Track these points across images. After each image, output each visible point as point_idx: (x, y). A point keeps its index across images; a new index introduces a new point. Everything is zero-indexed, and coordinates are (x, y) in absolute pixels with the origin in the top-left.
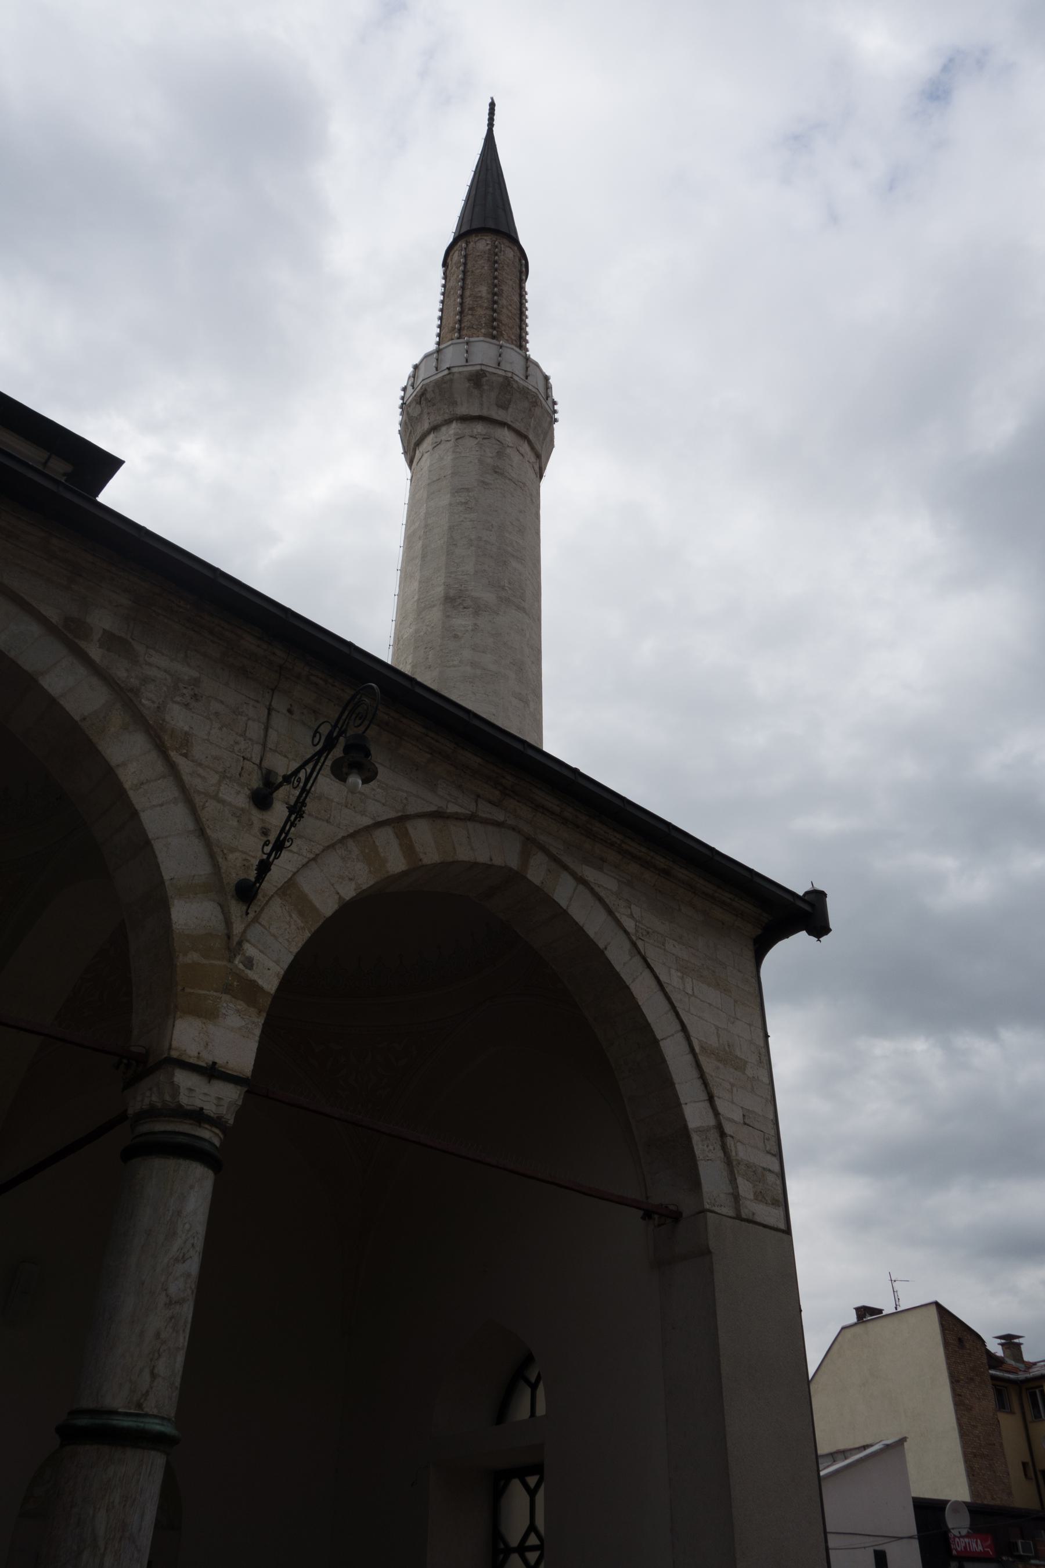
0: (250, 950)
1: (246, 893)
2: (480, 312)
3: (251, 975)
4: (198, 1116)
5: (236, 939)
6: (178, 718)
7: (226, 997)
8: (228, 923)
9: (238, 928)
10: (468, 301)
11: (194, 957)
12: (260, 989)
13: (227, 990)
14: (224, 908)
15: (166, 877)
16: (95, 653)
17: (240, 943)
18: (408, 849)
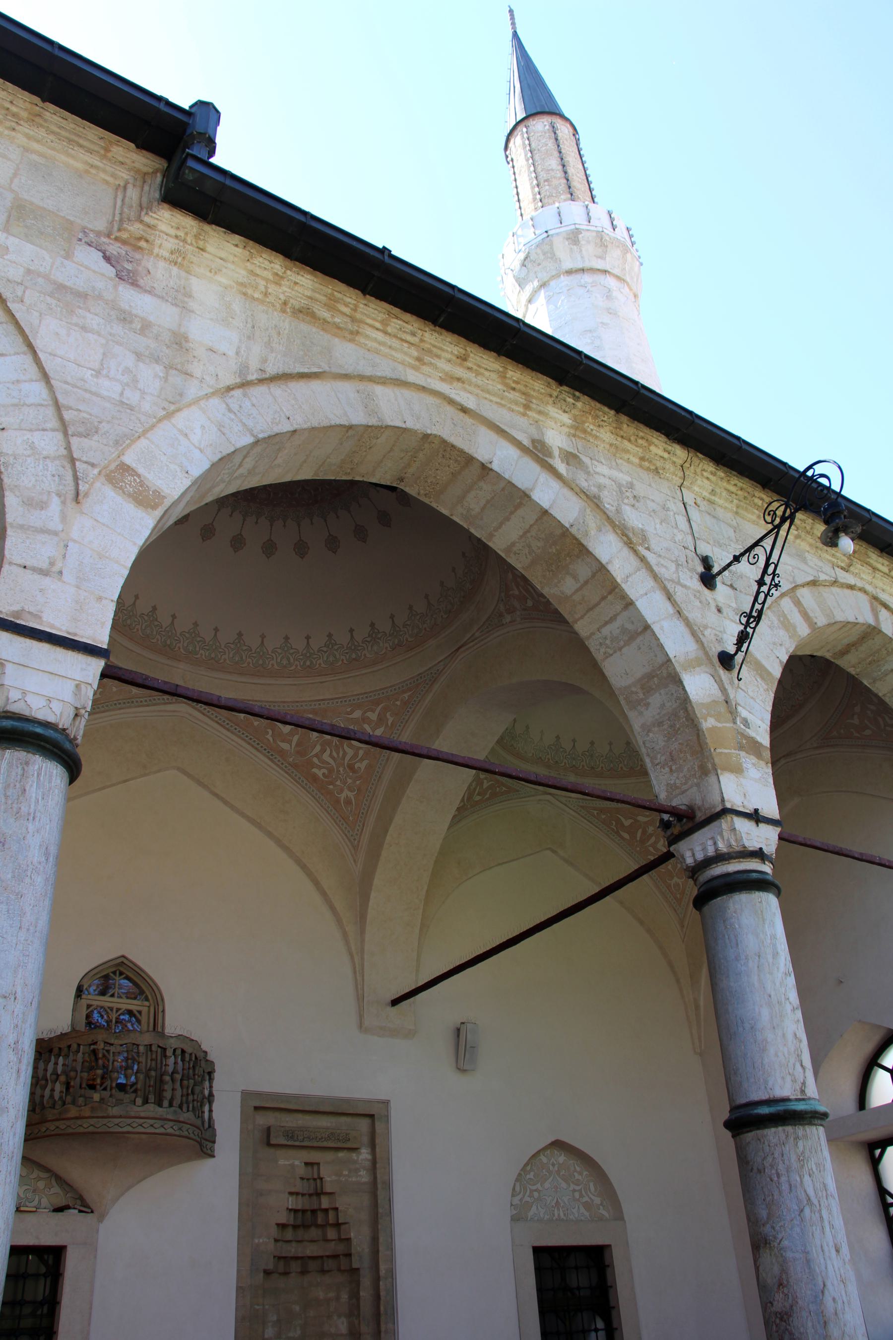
2: (555, 182)
4: (759, 854)
7: (743, 754)
10: (543, 175)
12: (760, 744)
13: (741, 748)
15: (671, 656)
16: (562, 468)
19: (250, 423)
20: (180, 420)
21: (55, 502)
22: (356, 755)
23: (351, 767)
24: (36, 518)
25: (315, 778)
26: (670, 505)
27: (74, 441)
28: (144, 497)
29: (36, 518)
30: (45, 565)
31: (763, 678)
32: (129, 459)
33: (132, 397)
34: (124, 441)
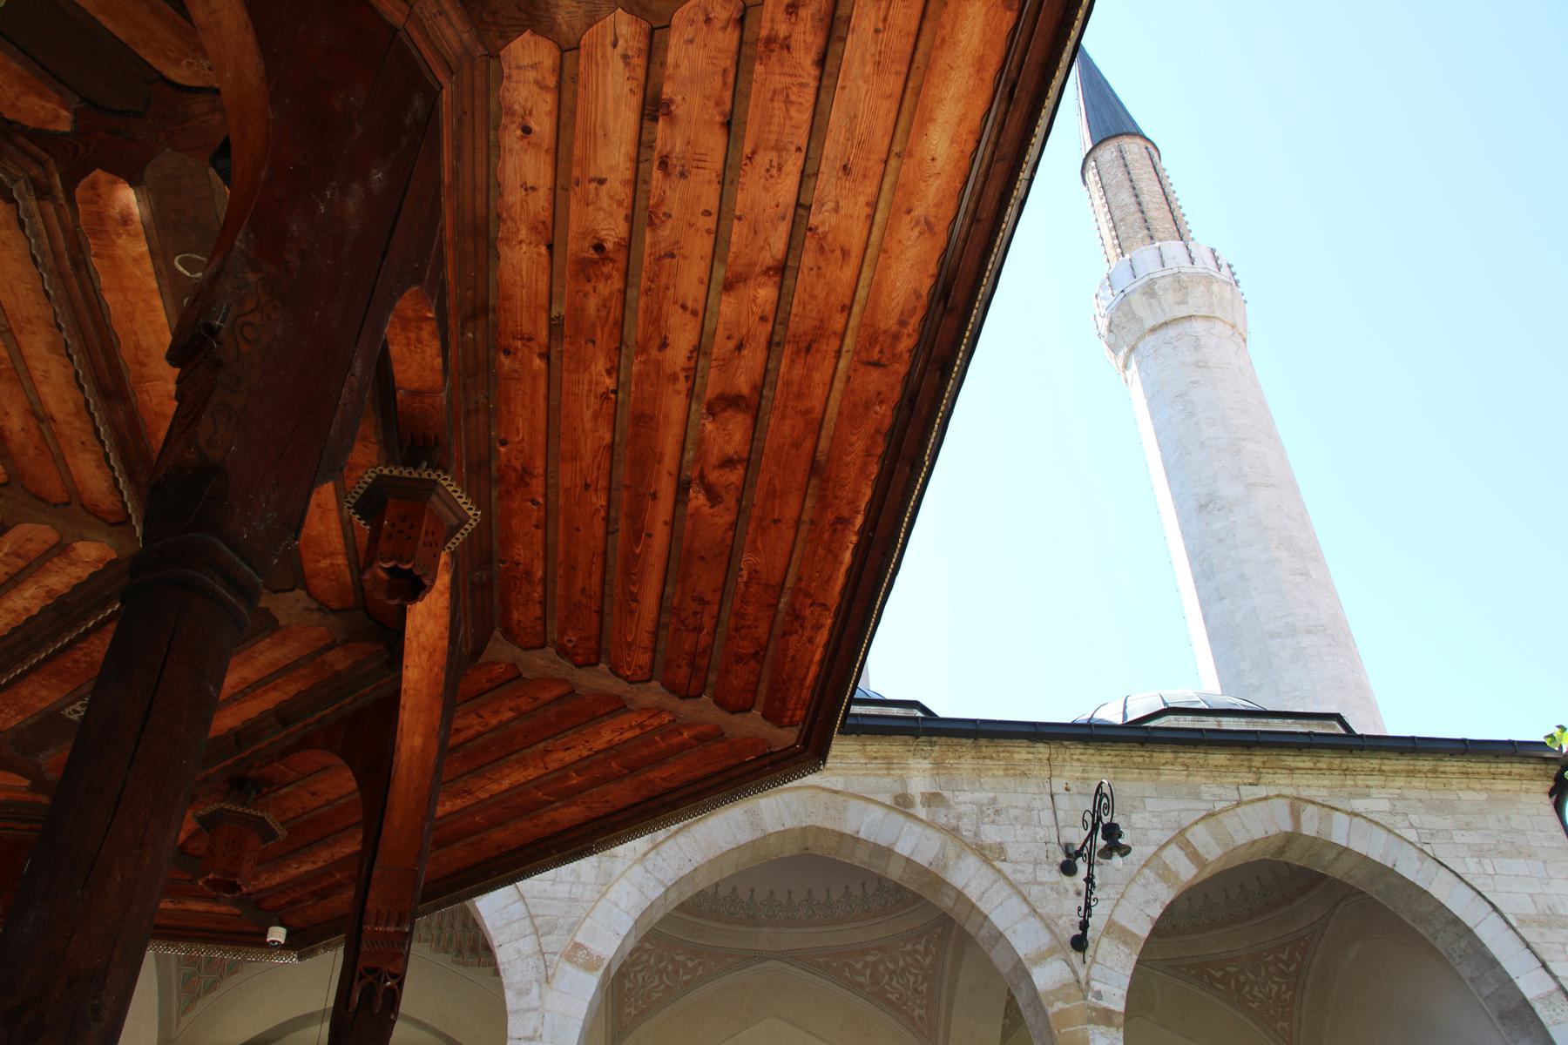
0: (1096, 986)
1: (1079, 943)
2: (1130, 219)
3: (1104, 1004)
5: (1083, 983)
6: (991, 835)
7: (1091, 1026)
8: (1074, 972)
9: (1082, 974)
10: (1118, 214)
11: (1059, 1005)
13: (1090, 1021)
14: (1070, 965)
15: (1021, 955)
17: (1088, 983)
18: (1194, 856)
19: (661, 877)
20: (612, 895)
21: (535, 986)
22: (916, 981)
23: (916, 990)
24: (525, 1003)
25: (890, 1002)
26: (1037, 804)
27: (543, 940)
28: (589, 966)
29: (525, 1003)
30: (530, 1033)
31: (1125, 943)
32: (579, 939)
33: (577, 891)
34: (572, 929)
